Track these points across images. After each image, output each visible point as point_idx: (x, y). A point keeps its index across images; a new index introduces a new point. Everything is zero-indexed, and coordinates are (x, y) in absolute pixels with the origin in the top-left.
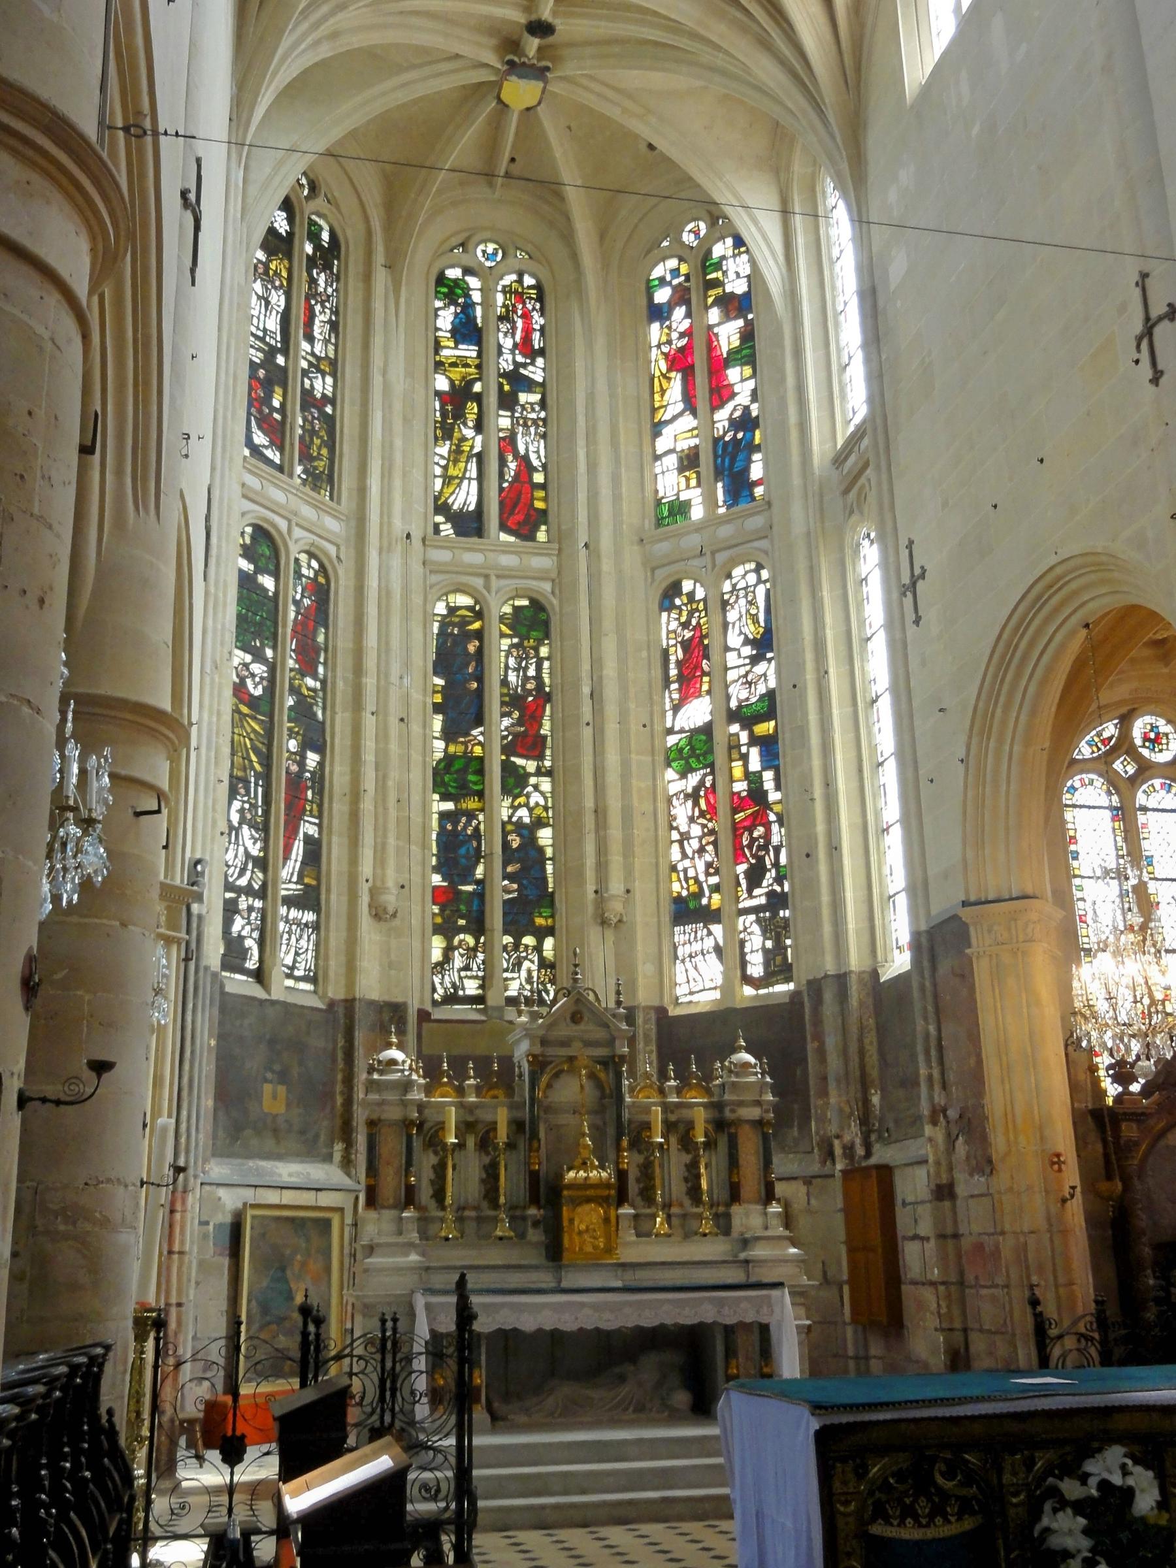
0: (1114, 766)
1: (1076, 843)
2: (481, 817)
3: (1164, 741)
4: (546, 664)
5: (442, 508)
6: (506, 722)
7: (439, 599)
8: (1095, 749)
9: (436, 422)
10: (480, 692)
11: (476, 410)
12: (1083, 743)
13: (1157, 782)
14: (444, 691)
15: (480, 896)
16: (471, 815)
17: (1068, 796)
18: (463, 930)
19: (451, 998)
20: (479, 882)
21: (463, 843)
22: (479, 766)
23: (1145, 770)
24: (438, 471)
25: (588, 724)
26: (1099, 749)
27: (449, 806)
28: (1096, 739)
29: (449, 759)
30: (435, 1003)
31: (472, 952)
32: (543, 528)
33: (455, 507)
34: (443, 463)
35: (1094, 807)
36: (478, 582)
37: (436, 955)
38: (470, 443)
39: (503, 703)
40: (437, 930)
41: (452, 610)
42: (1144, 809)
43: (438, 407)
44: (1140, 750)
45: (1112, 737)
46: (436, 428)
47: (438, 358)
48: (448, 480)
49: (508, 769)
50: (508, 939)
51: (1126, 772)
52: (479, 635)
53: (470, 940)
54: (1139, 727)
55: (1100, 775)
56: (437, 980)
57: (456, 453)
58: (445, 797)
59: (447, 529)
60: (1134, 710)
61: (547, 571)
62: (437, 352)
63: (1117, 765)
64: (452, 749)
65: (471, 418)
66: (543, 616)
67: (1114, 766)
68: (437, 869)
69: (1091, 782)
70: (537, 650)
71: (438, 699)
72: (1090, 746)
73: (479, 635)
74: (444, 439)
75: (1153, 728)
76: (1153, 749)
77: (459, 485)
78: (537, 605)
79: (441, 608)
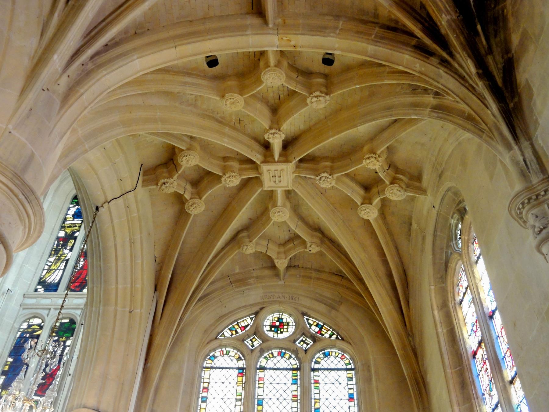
0: (246, 342)
1: (207, 392)
3: (285, 327)
4: (68, 348)
7: (25, 321)
8: (234, 332)
9: (53, 249)
11: (73, 243)
12: (227, 329)
13: (275, 352)
17: (209, 361)
25: (70, 375)
26: (237, 332)
28: (236, 327)
32: (87, 287)
33: (48, 282)
34: (50, 264)
35: (226, 368)
36: (44, 313)
38: (65, 255)
42: (263, 368)
43: (56, 243)
44: (266, 332)
45: (248, 325)
46: (52, 251)
47: (63, 225)
48: (49, 270)
51: (253, 346)
52: (38, 337)
54: (268, 320)
55: (235, 348)
57: (59, 259)
60: (261, 309)
61: (79, 305)
62: (64, 223)
63: (248, 342)
65: (69, 246)
66: (73, 326)
67: (246, 342)
69: (228, 353)
70: (65, 342)
71: (7, 368)
72: (230, 330)
74: (54, 255)
76: (277, 332)
77: (54, 273)
78: (72, 322)
79: (25, 326)
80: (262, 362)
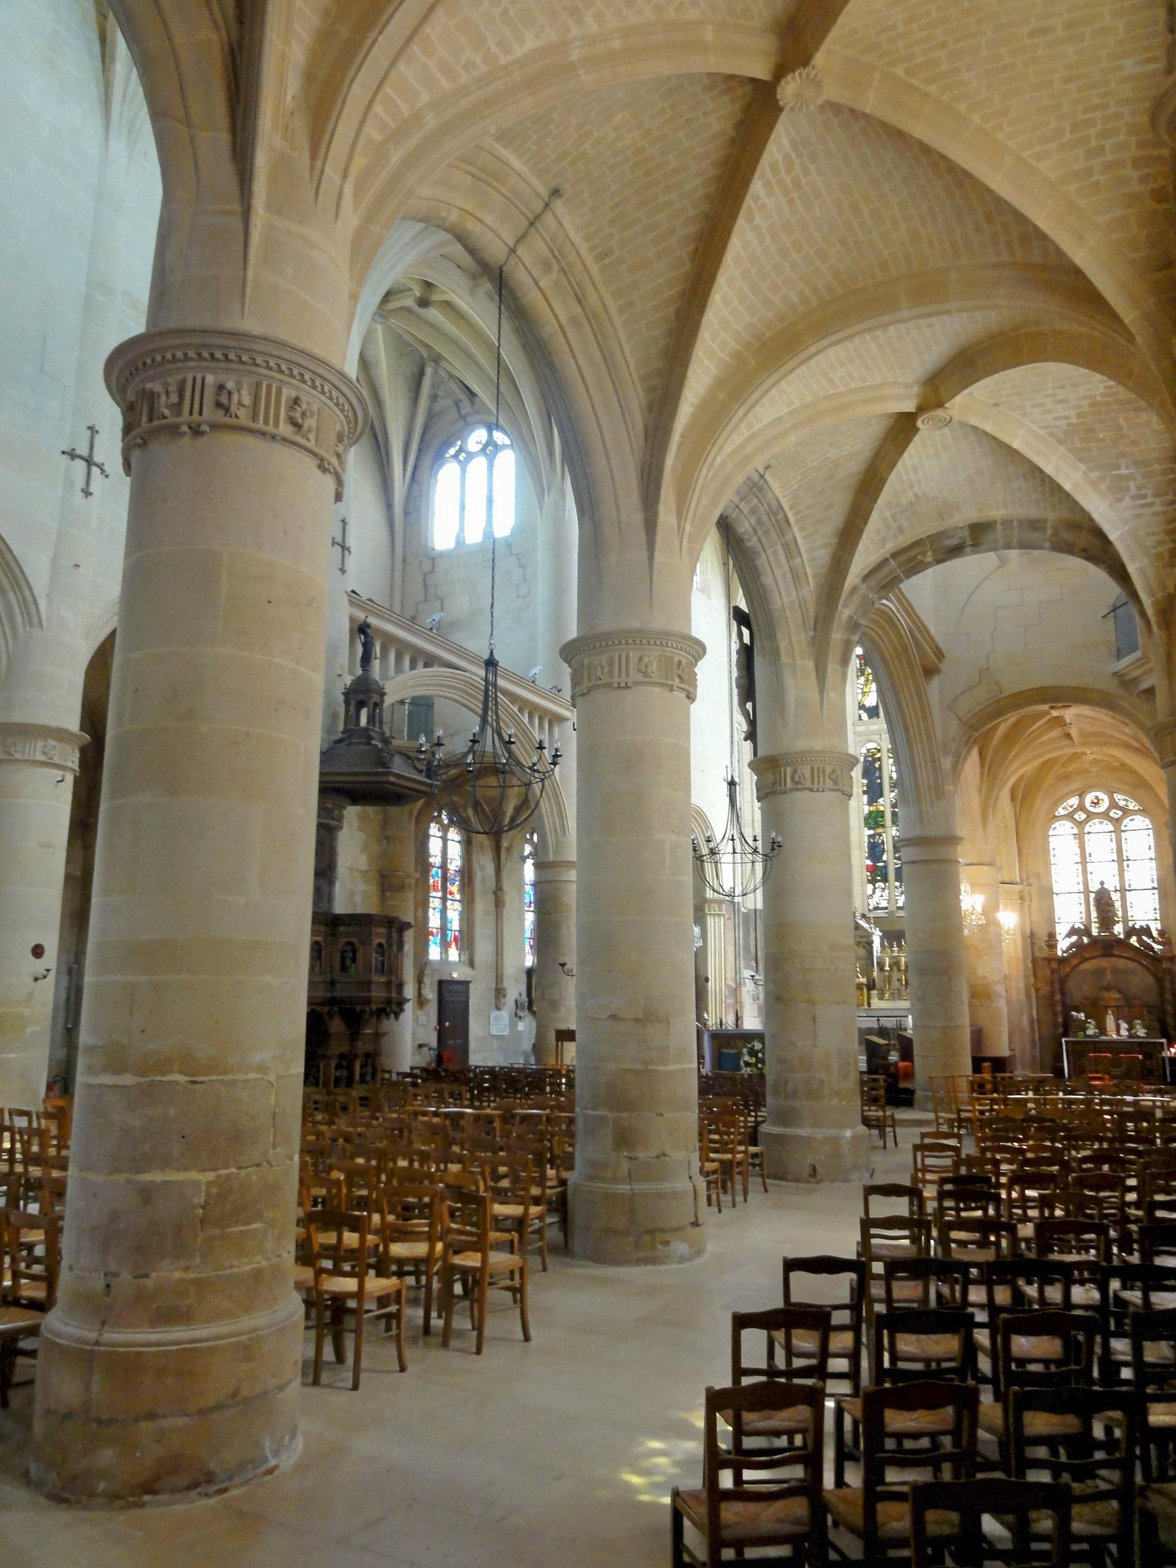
2: (884, 835)
5: (862, 707)
6: (893, 794)
10: (881, 784)
13: (1096, 821)
14: (867, 785)
15: (885, 867)
16: (880, 835)
18: (879, 881)
19: (876, 908)
20: (884, 862)
21: (877, 847)
22: (881, 814)
23: (1090, 816)
24: (860, 691)
27: (872, 832)
29: (871, 813)
30: (870, 910)
31: (883, 889)
37: (870, 892)
39: (891, 787)
40: (869, 882)
41: (868, 750)
42: (1089, 833)
48: (864, 694)
49: (894, 814)
50: (897, 884)
52: (879, 759)
53: (882, 885)
54: (1089, 798)
56: (870, 901)
58: (870, 829)
59: (865, 716)
63: (1076, 816)
64: (871, 809)
68: (867, 858)
71: (865, 788)
73: (879, 759)
75: (1097, 797)
79: (864, 751)
80: (1087, 829)
